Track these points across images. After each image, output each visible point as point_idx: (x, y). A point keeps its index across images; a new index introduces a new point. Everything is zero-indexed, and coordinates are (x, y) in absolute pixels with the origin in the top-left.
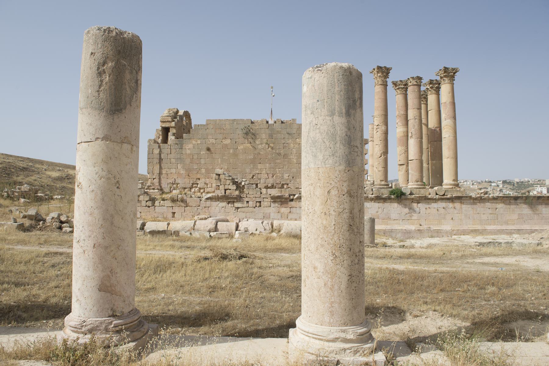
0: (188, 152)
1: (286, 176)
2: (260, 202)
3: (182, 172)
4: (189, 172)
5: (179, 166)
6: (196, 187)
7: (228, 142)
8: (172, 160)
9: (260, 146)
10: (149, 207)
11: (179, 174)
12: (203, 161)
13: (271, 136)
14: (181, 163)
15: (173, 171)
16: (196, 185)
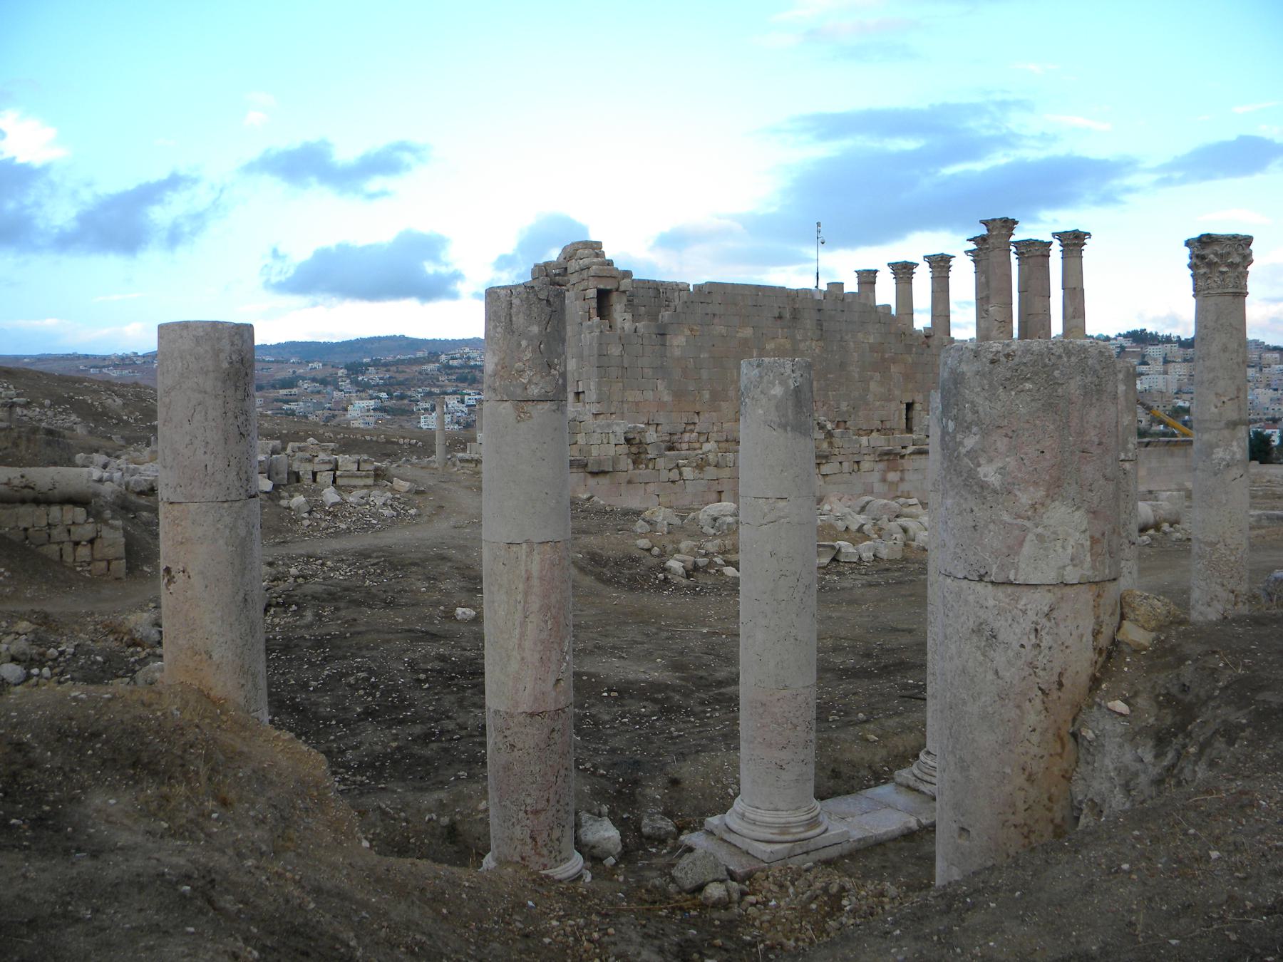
0: (677, 352)
1: (844, 407)
2: (858, 463)
3: (667, 398)
4: (679, 395)
5: (661, 385)
6: (692, 431)
7: (748, 332)
8: (646, 370)
9: (802, 346)
10: (673, 482)
11: (661, 405)
12: (705, 374)
13: (820, 324)
14: (663, 379)
15: (649, 395)
16: (692, 427)
